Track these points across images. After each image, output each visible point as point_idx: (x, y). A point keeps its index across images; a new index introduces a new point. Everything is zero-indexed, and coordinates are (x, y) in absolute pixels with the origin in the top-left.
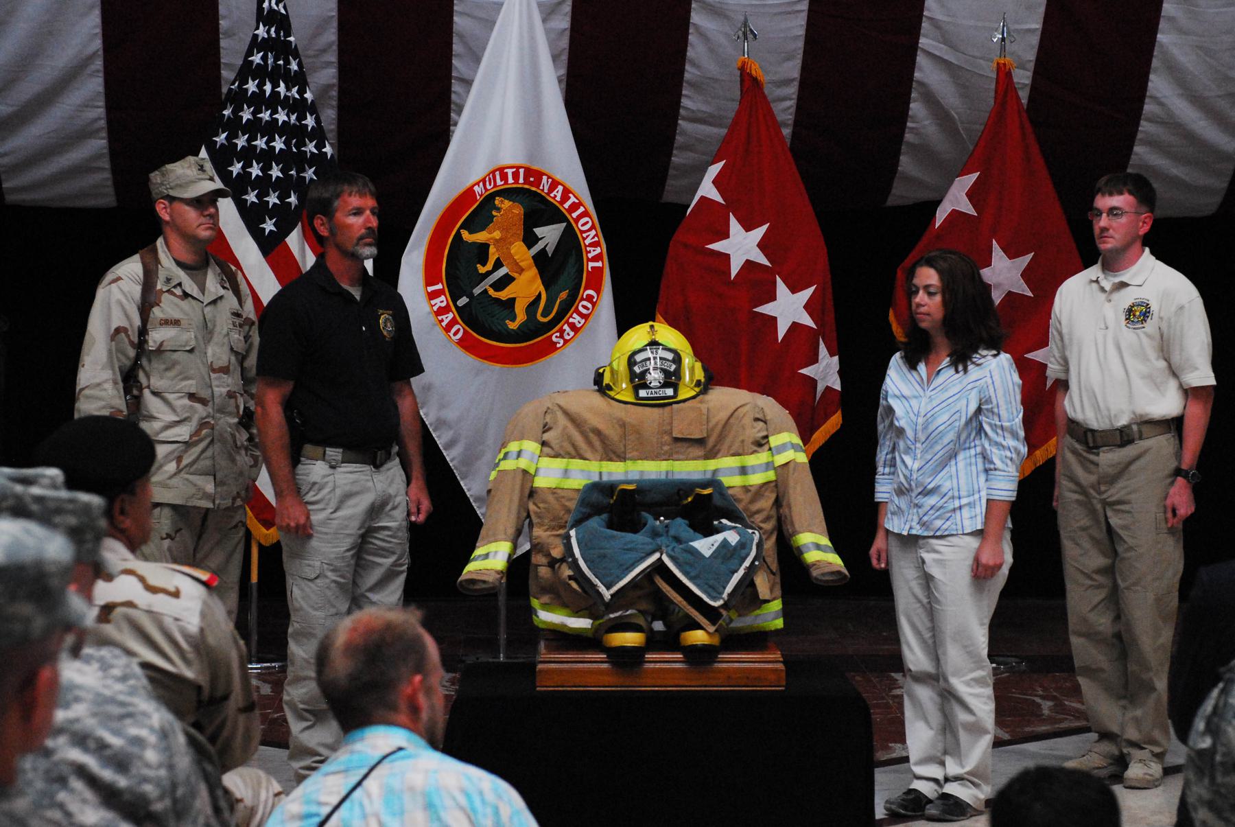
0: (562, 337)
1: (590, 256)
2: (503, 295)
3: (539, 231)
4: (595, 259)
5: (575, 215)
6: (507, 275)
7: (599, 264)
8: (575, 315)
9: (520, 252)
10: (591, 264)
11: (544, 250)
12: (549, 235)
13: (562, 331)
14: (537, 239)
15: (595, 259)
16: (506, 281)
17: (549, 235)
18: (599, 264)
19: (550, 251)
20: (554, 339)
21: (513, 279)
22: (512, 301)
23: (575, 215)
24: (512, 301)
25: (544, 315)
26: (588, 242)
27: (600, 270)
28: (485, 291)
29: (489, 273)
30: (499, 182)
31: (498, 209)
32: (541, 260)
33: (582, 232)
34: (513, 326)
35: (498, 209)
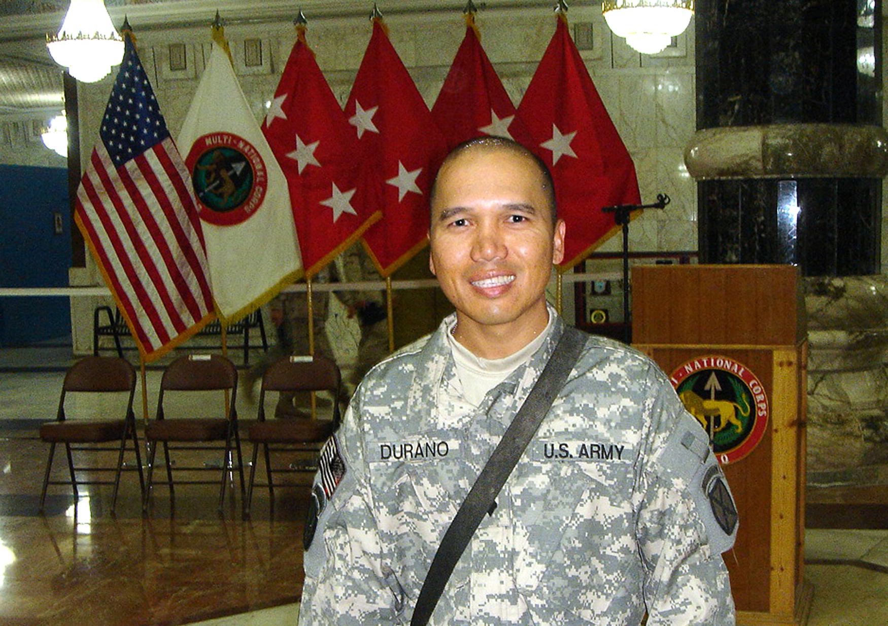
2: (723, 424)
4: (739, 369)
9: (710, 404)
12: (713, 383)
14: (709, 392)
15: (739, 369)
17: (713, 383)
19: (719, 388)
20: (760, 415)
21: (719, 416)
22: (729, 425)
24: (729, 425)
26: (728, 367)
28: (715, 433)
32: (719, 396)
34: (740, 430)
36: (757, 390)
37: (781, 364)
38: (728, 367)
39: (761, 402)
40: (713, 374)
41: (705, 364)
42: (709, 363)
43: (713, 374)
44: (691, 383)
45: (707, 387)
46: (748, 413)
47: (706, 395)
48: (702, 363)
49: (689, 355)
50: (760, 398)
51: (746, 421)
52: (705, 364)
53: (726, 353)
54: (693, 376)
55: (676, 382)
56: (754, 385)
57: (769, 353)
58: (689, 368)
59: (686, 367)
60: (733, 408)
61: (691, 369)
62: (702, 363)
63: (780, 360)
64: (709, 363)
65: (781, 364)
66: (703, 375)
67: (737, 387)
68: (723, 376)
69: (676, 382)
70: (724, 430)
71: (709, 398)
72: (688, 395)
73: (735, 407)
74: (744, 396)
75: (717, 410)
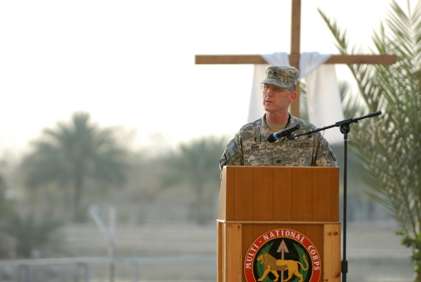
0: (317, 266)
1: (298, 239)
2: (290, 277)
3: (279, 251)
4: (300, 239)
5: (282, 235)
6: (284, 272)
7: (303, 238)
8: (313, 257)
10: (301, 241)
11: (285, 254)
12: (283, 248)
13: (315, 265)
14: (280, 253)
15: (300, 239)
16: (286, 273)
17: (283, 248)
18: (303, 238)
19: (287, 251)
20: (316, 269)
21: (287, 271)
22: (294, 277)
23: (282, 235)
24: (294, 277)
25: (305, 268)
26: (294, 237)
29: (280, 278)
30: (253, 255)
31: (261, 261)
32: (288, 257)
35: (261, 261)
36: (313, 252)
38: (294, 237)
39: (316, 261)
40: (283, 242)
41: (278, 235)
43: (283, 242)
44: (268, 248)
45: (279, 251)
46: (307, 269)
47: (278, 256)
50: (315, 258)
51: (306, 275)
52: (278, 235)
56: (311, 249)
59: (264, 237)
60: (297, 266)
61: (268, 238)
66: (276, 242)
67: (299, 249)
68: (290, 242)
69: (257, 247)
70: (290, 280)
71: (280, 258)
72: (266, 256)
73: (299, 265)
74: (304, 256)
75: (286, 266)
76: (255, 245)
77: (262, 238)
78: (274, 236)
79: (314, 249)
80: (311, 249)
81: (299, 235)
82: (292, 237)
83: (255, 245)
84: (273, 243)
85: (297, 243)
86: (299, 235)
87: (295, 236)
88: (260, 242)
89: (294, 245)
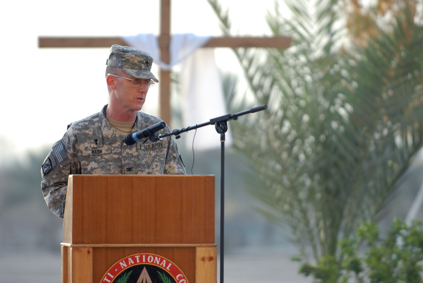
1: (164, 266)
4: (167, 265)
5: (144, 261)
7: (170, 265)
10: (168, 268)
15: (167, 265)
18: (170, 265)
23: (144, 261)
26: (158, 263)
27: (172, 265)
33: (153, 263)
37: (203, 259)
38: (158, 263)
41: (138, 261)
42: (141, 259)
48: (135, 260)
49: (124, 252)
52: (138, 261)
53: (155, 250)
54: (127, 271)
55: (112, 277)
56: (180, 278)
57: (194, 248)
58: (123, 265)
59: (121, 263)
61: (125, 266)
62: (135, 260)
63: (202, 256)
64: (141, 259)
65: (203, 259)
68: (153, 271)
69: (112, 277)
76: (109, 274)
77: (118, 266)
78: (133, 263)
79: (184, 278)
80: (180, 278)
81: (165, 261)
82: (156, 264)
83: (109, 274)
84: (131, 272)
85: (162, 271)
86: (165, 261)
87: (160, 262)
88: (116, 270)
89: (158, 274)
